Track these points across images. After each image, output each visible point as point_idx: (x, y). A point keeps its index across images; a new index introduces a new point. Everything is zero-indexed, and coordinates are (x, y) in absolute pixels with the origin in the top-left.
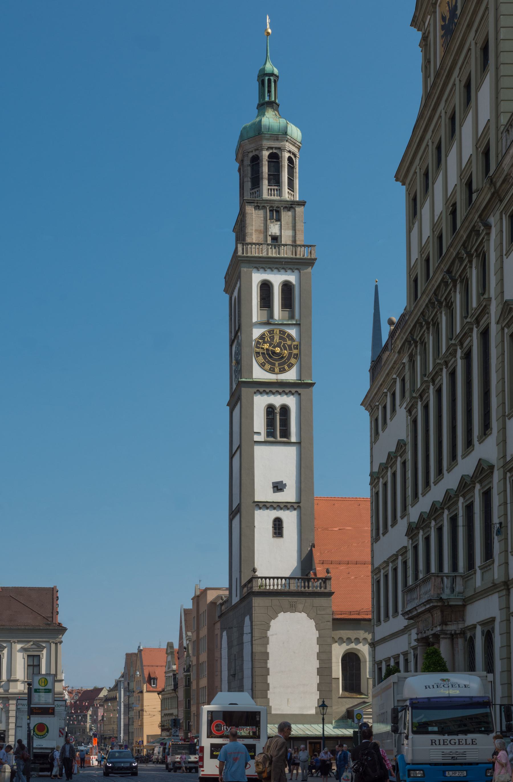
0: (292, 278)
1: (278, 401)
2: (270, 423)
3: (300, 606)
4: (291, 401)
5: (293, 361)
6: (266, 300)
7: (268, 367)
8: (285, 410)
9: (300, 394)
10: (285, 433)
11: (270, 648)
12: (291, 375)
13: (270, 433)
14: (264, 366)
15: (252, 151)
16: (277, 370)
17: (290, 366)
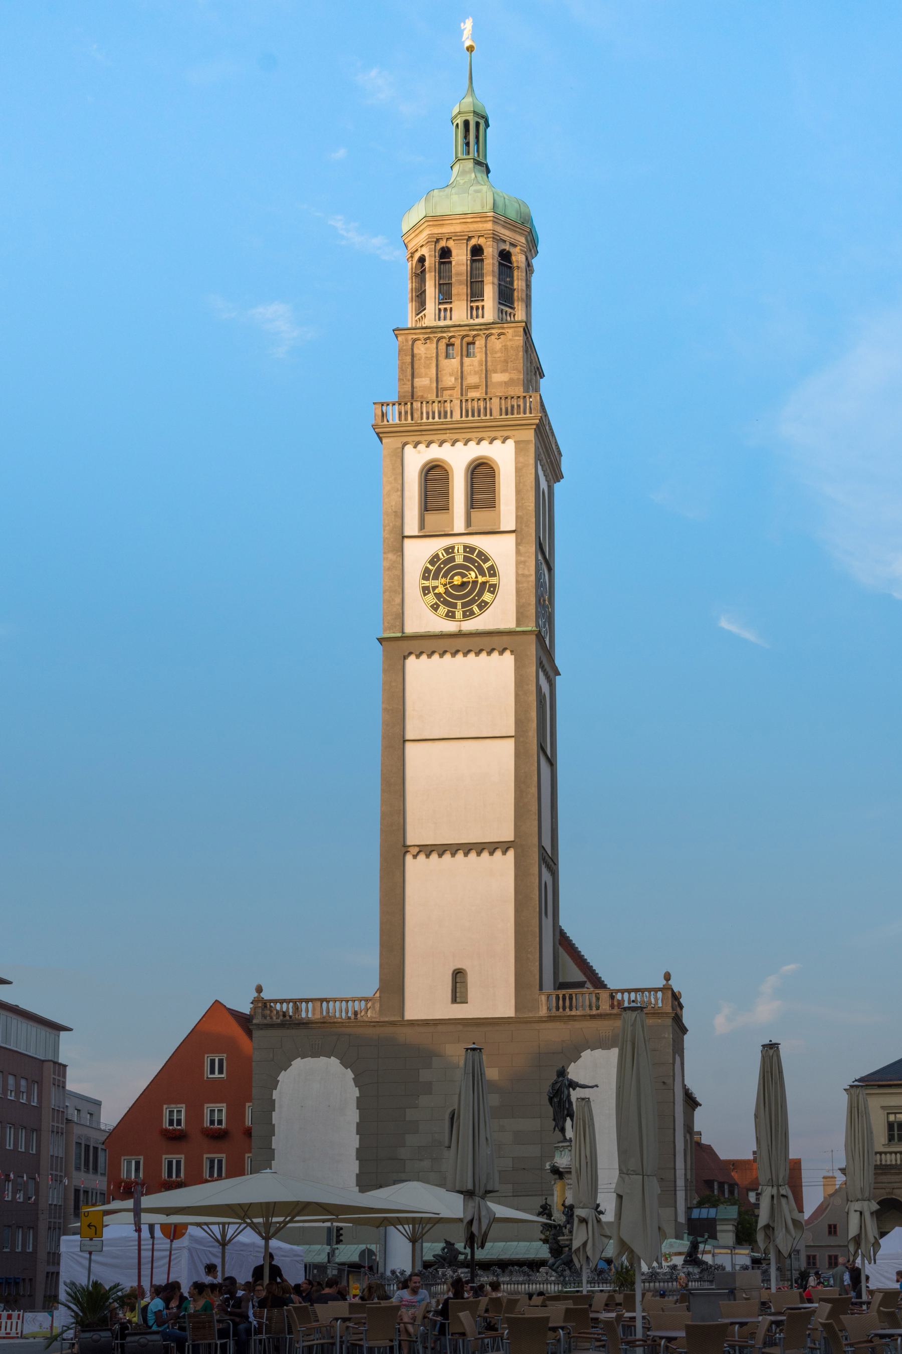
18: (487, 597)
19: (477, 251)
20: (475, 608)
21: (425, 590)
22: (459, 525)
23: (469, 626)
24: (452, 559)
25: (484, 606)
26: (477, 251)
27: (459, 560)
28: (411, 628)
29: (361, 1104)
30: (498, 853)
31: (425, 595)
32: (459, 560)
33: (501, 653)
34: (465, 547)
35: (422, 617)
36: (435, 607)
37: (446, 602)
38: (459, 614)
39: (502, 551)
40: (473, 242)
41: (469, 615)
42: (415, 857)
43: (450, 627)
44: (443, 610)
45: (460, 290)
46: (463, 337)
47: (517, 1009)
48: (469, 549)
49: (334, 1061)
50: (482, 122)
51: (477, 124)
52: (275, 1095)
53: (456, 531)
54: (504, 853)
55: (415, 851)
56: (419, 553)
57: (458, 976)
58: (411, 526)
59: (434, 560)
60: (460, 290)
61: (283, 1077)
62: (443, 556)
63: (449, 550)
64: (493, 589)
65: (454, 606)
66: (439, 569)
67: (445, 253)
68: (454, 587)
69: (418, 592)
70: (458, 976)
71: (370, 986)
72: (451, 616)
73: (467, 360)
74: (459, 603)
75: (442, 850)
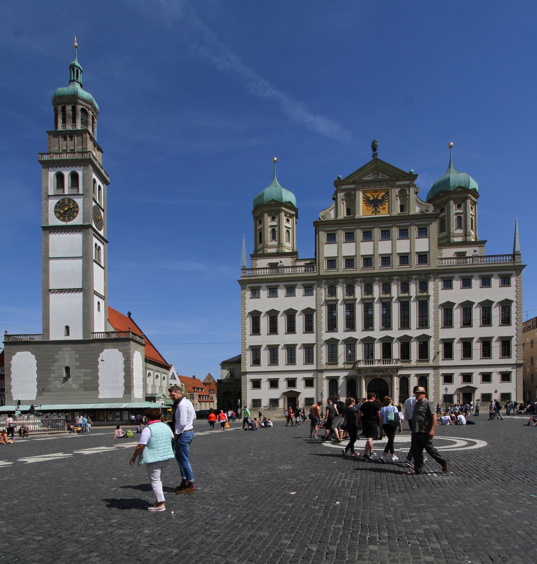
18: (75, 214)
19: (74, 109)
20: (71, 218)
21: (56, 212)
24: (64, 203)
25: (74, 217)
26: (74, 109)
27: (66, 203)
28: (51, 223)
29: (38, 365)
32: (66, 203)
34: (68, 199)
35: (54, 221)
36: (59, 218)
37: (61, 216)
38: (66, 220)
39: (79, 201)
41: (70, 220)
43: (64, 223)
44: (61, 218)
47: (84, 336)
48: (70, 200)
49: (29, 353)
50: (79, 71)
51: (77, 71)
52: (11, 362)
53: (66, 194)
57: (67, 328)
58: (51, 193)
59: (58, 203)
60: (69, 120)
61: (14, 357)
62: (61, 202)
63: (63, 200)
64: (77, 212)
65: (65, 217)
66: (60, 206)
67: (64, 109)
68: (66, 211)
69: (53, 213)
70: (67, 328)
71: (39, 330)
72: (64, 220)
74: (66, 216)
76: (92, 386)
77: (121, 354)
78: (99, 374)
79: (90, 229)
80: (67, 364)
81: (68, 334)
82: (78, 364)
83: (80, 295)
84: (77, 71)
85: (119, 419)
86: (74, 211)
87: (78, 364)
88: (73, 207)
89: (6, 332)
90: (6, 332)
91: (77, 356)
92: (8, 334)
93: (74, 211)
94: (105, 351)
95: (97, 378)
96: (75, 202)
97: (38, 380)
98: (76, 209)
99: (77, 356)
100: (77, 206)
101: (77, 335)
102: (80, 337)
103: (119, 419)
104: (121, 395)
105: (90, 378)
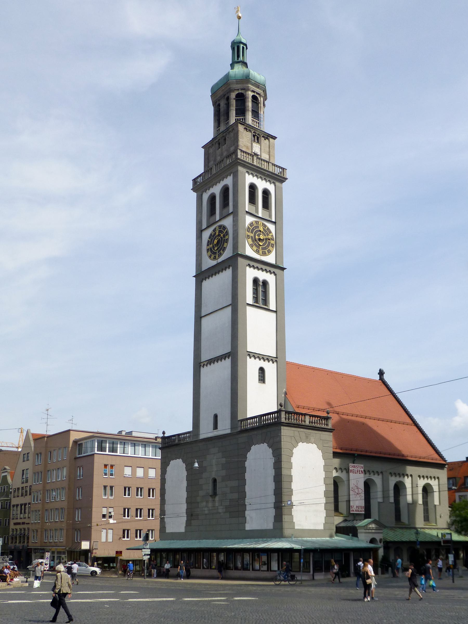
0: (271, 188)
1: (262, 276)
2: (255, 291)
3: (313, 440)
4: (271, 279)
5: (270, 248)
6: (253, 199)
7: (255, 248)
8: (265, 283)
9: (275, 275)
10: (266, 301)
11: (295, 472)
12: (271, 258)
13: (256, 299)
14: (252, 246)
15: (238, 90)
16: (261, 252)
17: (270, 252)
19: (228, 99)
21: (208, 250)
22: (218, 218)
23: (220, 260)
25: (224, 249)
30: (227, 359)
31: (208, 252)
33: (229, 268)
36: (210, 257)
40: (226, 97)
41: (220, 255)
42: (203, 367)
43: (214, 263)
45: (222, 118)
46: (222, 138)
47: (232, 429)
48: (220, 227)
54: (229, 358)
55: (202, 364)
56: (206, 235)
57: (216, 417)
63: (214, 230)
64: (227, 241)
67: (219, 105)
70: (216, 417)
72: (215, 258)
73: (224, 147)
75: (211, 361)
76: (238, 508)
77: (270, 451)
78: (247, 488)
79: (240, 260)
80: (214, 476)
81: (216, 427)
82: (223, 473)
83: (227, 363)
84: (238, 47)
85: (265, 568)
86: (224, 240)
87: (223, 473)
88: (224, 236)
89: (164, 433)
90: (164, 433)
91: (224, 460)
92: (166, 435)
93: (224, 240)
94: (253, 448)
95: (243, 495)
96: (224, 228)
97: (187, 502)
98: (227, 237)
99: (224, 460)
100: (227, 233)
101: (225, 427)
102: (229, 431)
103: (265, 568)
104: (269, 525)
105: (235, 496)
